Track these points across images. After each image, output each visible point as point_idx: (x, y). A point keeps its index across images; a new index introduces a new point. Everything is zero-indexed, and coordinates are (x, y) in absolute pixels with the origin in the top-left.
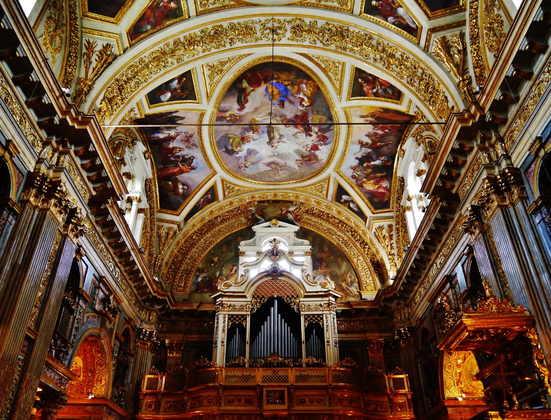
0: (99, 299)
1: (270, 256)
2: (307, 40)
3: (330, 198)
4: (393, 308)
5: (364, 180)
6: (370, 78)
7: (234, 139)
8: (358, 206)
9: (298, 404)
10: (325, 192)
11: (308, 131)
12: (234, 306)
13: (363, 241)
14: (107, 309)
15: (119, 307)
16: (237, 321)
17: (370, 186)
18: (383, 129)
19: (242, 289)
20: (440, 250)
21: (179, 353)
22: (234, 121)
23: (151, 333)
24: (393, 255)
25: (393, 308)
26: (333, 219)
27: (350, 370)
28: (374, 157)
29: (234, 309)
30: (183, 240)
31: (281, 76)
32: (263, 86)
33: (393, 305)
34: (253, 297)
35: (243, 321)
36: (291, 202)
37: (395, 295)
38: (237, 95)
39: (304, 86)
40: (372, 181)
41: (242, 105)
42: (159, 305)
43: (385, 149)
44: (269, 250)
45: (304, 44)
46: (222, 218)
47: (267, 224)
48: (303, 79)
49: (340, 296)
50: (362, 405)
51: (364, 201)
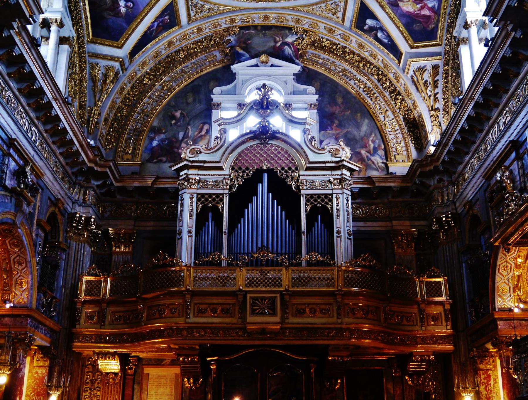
0: (10, 171)
1: (257, 110)
3: (347, 23)
4: (432, 188)
8: (389, 37)
9: (295, 316)
10: (340, 14)
12: (206, 181)
13: (395, 89)
14: (22, 186)
15: (40, 182)
16: (210, 202)
19: (216, 157)
20: (506, 105)
21: (129, 247)
23: (88, 219)
24: (437, 110)
25: (432, 188)
26: (352, 56)
27: (367, 270)
29: (206, 187)
30: (129, 86)
33: (433, 182)
34: (233, 169)
35: (218, 203)
36: (290, 29)
37: (436, 168)
42: (97, 180)
44: (256, 100)
46: (185, 52)
47: (254, 61)
49: (357, 169)
50: (383, 316)
51: (398, 28)
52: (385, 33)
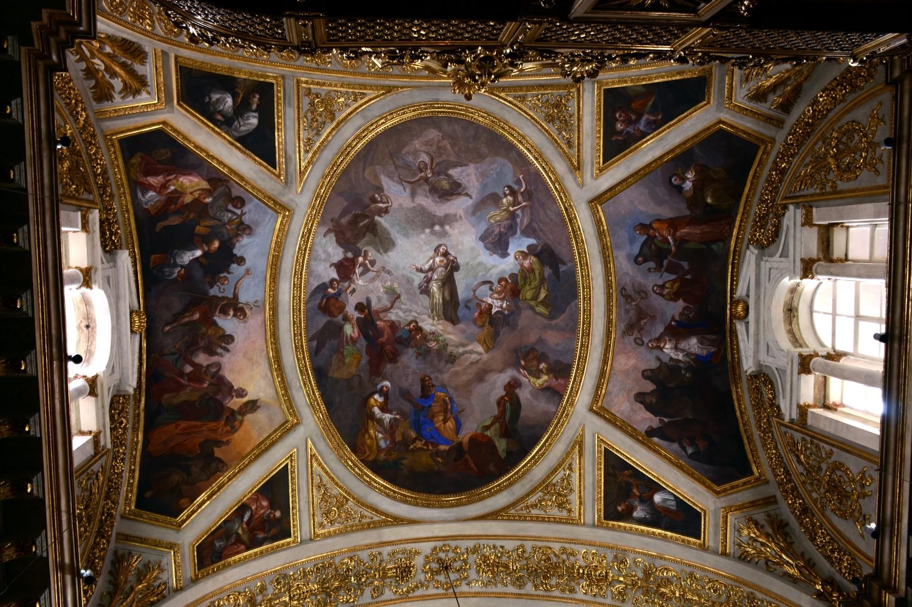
2: (386, 557)
5: (209, 200)
6: (261, 536)
7: (535, 298)
11: (368, 317)
17: (191, 184)
18: (199, 374)
22: (528, 357)
28: (198, 273)
31: (430, 461)
32: (465, 436)
38: (520, 422)
39: (383, 444)
40: (188, 199)
41: (510, 398)
43: (177, 305)
45: (389, 549)
48: (385, 460)
52: (219, 117)
